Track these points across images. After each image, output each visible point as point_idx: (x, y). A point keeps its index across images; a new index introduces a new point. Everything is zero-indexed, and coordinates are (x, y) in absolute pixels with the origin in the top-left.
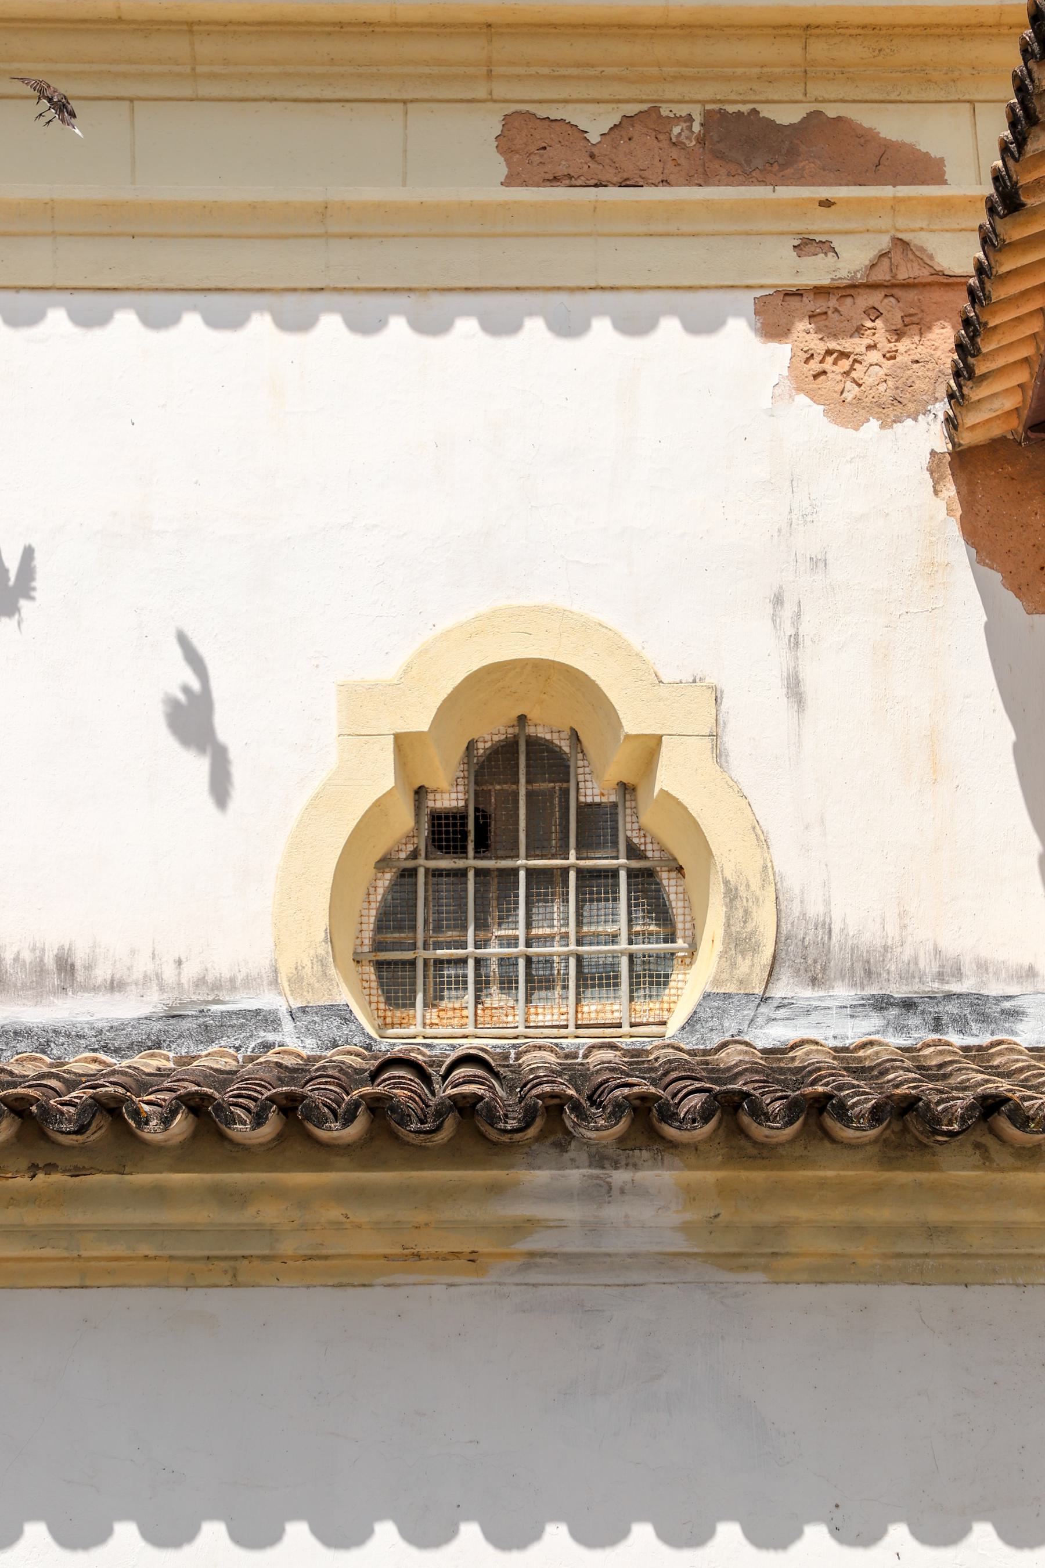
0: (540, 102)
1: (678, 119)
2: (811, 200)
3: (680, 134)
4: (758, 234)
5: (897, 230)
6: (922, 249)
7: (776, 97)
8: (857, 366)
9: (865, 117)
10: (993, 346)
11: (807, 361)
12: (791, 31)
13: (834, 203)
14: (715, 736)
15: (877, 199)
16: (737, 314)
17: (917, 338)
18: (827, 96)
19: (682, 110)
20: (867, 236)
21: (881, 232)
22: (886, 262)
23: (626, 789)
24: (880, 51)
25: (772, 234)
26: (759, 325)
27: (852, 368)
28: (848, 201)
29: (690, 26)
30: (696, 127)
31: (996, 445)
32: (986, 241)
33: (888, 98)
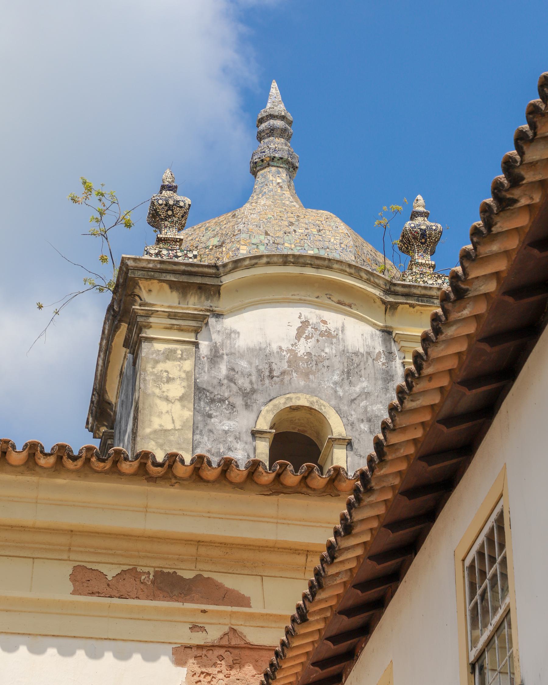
0: (89, 562)
1: (144, 573)
2: (198, 609)
3: (144, 579)
4: (175, 622)
5: (232, 625)
6: (242, 633)
7: (184, 568)
8: (213, 679)
9: (219, 578)
10: (281, 676)
11: (193, 676)
12: (192, 543)
13: (207, 612)
15: (225, 611)
16: (165, 654)
17: (238, 670)
18: (204, 569)
19: (146, 570)
20: (219, 626)
21: (225, 624)
22: (226, 637)
24: (227, 553)
25: (181, 622)
26: (174, 659)
27: (212, 680)
28: (213, 611)
29: (152, 537)
30: (151, 577)
32: (288, 632)
33: (229, 572)
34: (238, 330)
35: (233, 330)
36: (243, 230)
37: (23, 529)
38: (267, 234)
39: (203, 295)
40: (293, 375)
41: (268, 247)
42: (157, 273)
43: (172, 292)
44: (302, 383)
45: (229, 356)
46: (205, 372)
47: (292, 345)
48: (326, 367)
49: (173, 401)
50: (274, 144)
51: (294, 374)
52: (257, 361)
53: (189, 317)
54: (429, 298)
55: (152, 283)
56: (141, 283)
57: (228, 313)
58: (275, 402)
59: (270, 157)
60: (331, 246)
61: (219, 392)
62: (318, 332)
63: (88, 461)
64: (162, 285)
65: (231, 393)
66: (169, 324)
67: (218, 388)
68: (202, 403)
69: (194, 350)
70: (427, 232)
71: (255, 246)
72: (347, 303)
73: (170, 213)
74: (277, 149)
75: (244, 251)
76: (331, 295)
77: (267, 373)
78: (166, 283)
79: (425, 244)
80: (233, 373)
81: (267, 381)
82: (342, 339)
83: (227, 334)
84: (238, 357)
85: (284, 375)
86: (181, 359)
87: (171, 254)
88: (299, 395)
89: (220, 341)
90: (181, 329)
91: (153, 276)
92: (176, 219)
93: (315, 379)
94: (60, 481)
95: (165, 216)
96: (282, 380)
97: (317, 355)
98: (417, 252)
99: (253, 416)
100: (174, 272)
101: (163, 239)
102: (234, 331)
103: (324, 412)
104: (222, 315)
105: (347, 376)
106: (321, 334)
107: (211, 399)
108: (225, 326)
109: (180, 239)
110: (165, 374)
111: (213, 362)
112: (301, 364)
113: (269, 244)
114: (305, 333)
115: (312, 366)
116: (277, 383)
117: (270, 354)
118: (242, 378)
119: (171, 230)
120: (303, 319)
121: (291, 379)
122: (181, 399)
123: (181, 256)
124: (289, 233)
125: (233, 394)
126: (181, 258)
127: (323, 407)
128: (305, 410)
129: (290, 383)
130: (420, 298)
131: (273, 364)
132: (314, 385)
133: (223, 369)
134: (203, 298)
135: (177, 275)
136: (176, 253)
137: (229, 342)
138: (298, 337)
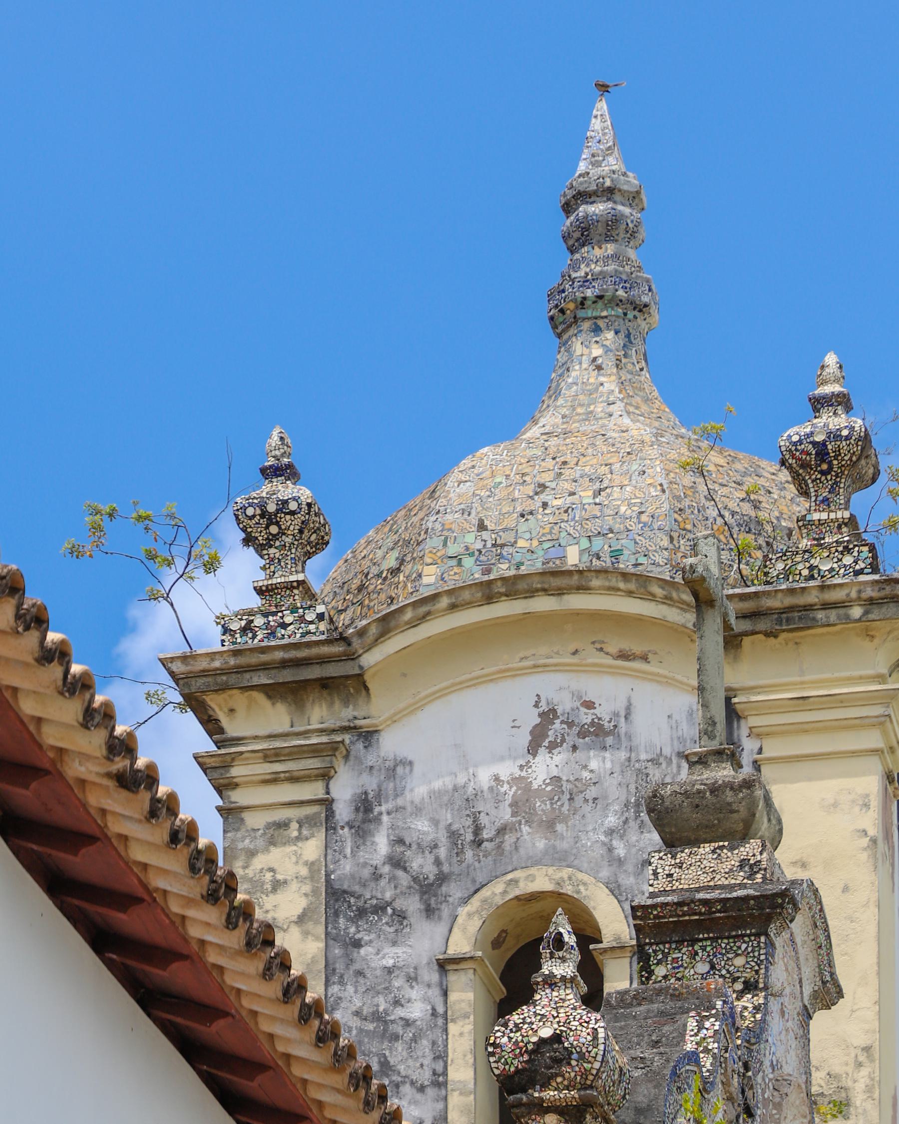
34: (409, 758)
35: (399, 759)
36: (433, 529)
38: (482, 527)
39: (336, 699)
40: (521, 832)
41: (482, 558)
42: (234, 676)
43: (273, 704)
44: (541, 844)
45: (393, 815)
46: (345, 857)
47: (521, 767)
48: (591, 801)
49: (285, 927)
50: (588, 265)
51: (525, 829)
52: (449, 816)
53: (304, 752)
54: (805, 610)
55: (231, 696)
56: (211, 700)
57: (389, 726)
58: (485, 893)
59: (574, 301)
60: (617, 526)
61: (374, 893)
62: (575, 730)
64: (251, 695)
65: (398, 891)
66: (269, 773)
67: (373, 884)
68: (342, 921)
69: (323, 815)
70: (830, 447)
71: (454, 562)
72: (638, 653)
73: (274, 529)
74: (589, 277)
75: (430, 577)
76: (603, 642)
77: (469, 837)
78: (257, 690)
79: (830, 473)
80: (402, 849)
81: (469, 854)
82: (626, 734)
83: (388, 770)
84: (411, 815)
85: (504, 834)
86: (298, 838)
87: (272, 623)
88: (533, 871)
89: (375, 786)
90: (294, 779)
91: (227, 682)
92: (288, 540)
93: (567, 830)
95: (267, 539)
96: (499, 847)
97: (572, 779)
98: (813, 494)
100: (264, 667)
101: (264, 588)
102: (401, 760)
103: (585, 897)
104: (376, 731)
105: (635, 812)
106: (582, 734)
107: (358, 909)
108: (382, 754)
109: (297, 581)
110: (269, 876)
111: (361, 834)
112: (538, 804)
113: (483, 551)
114: (548, 736)
115: (562, 805)
116: (490, 854)
117: (476, 795)
118: (420, 855)
119: (282, 564)
120: (544, 707)
121: (518, 839)
122: (301, 919)
123: (291, 624)
124: (531, 513)
125: (401, 892)
126: (292, 626)
127: (582, 888)
128: (552, 897)
129: (516, 848)
130: (784, 616)
131: (482, 814)
132: (564, 845)
133: (381, 844)
134: (337, 704)
135: (273, 672)
136: (282, 618)
137: (391, 785)
138: (533, 749)
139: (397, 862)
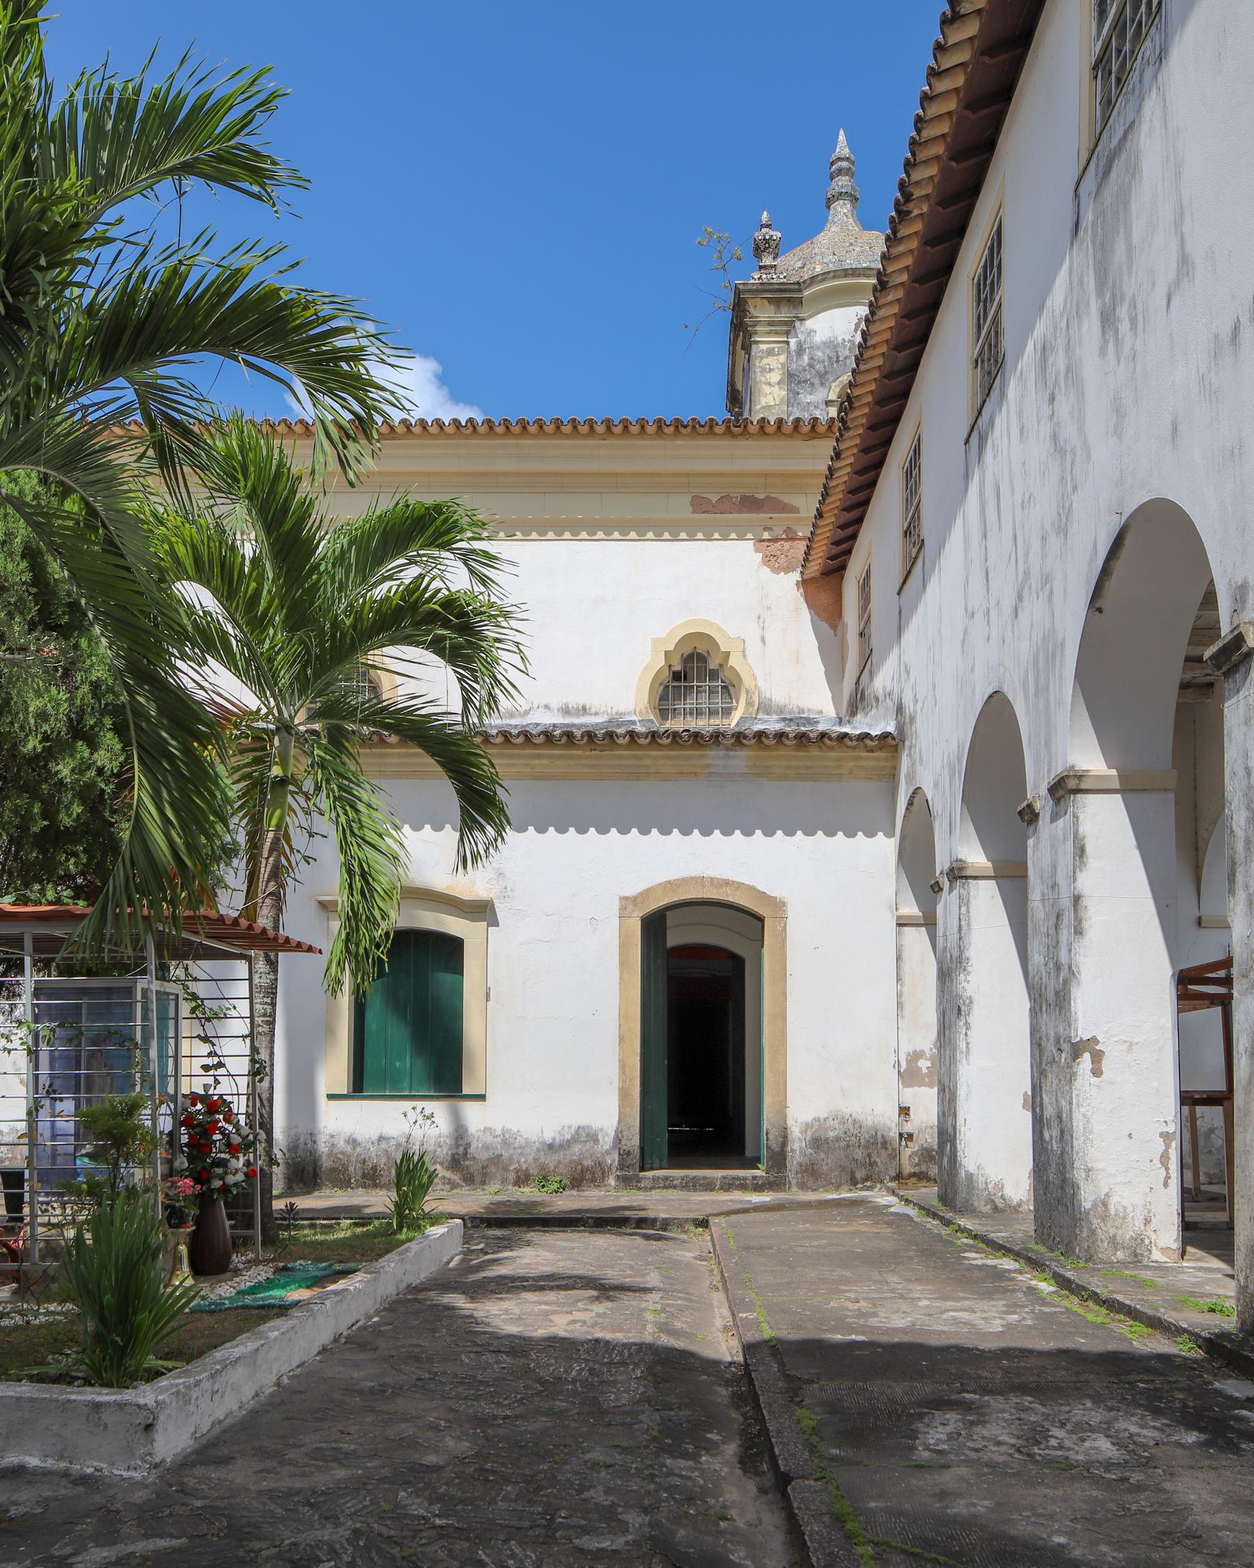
9: (778, 496)
14: (744, 651)
23: (721, 665)
31: (812, 580)
37: (659, 474)
63: (694, 427)
90: (777, 333)
94: (678, 442)
99: (826, 390)
122: (779, 383)
133: (806, 359)
139: (811, 366)
